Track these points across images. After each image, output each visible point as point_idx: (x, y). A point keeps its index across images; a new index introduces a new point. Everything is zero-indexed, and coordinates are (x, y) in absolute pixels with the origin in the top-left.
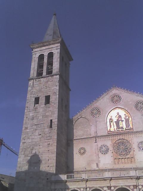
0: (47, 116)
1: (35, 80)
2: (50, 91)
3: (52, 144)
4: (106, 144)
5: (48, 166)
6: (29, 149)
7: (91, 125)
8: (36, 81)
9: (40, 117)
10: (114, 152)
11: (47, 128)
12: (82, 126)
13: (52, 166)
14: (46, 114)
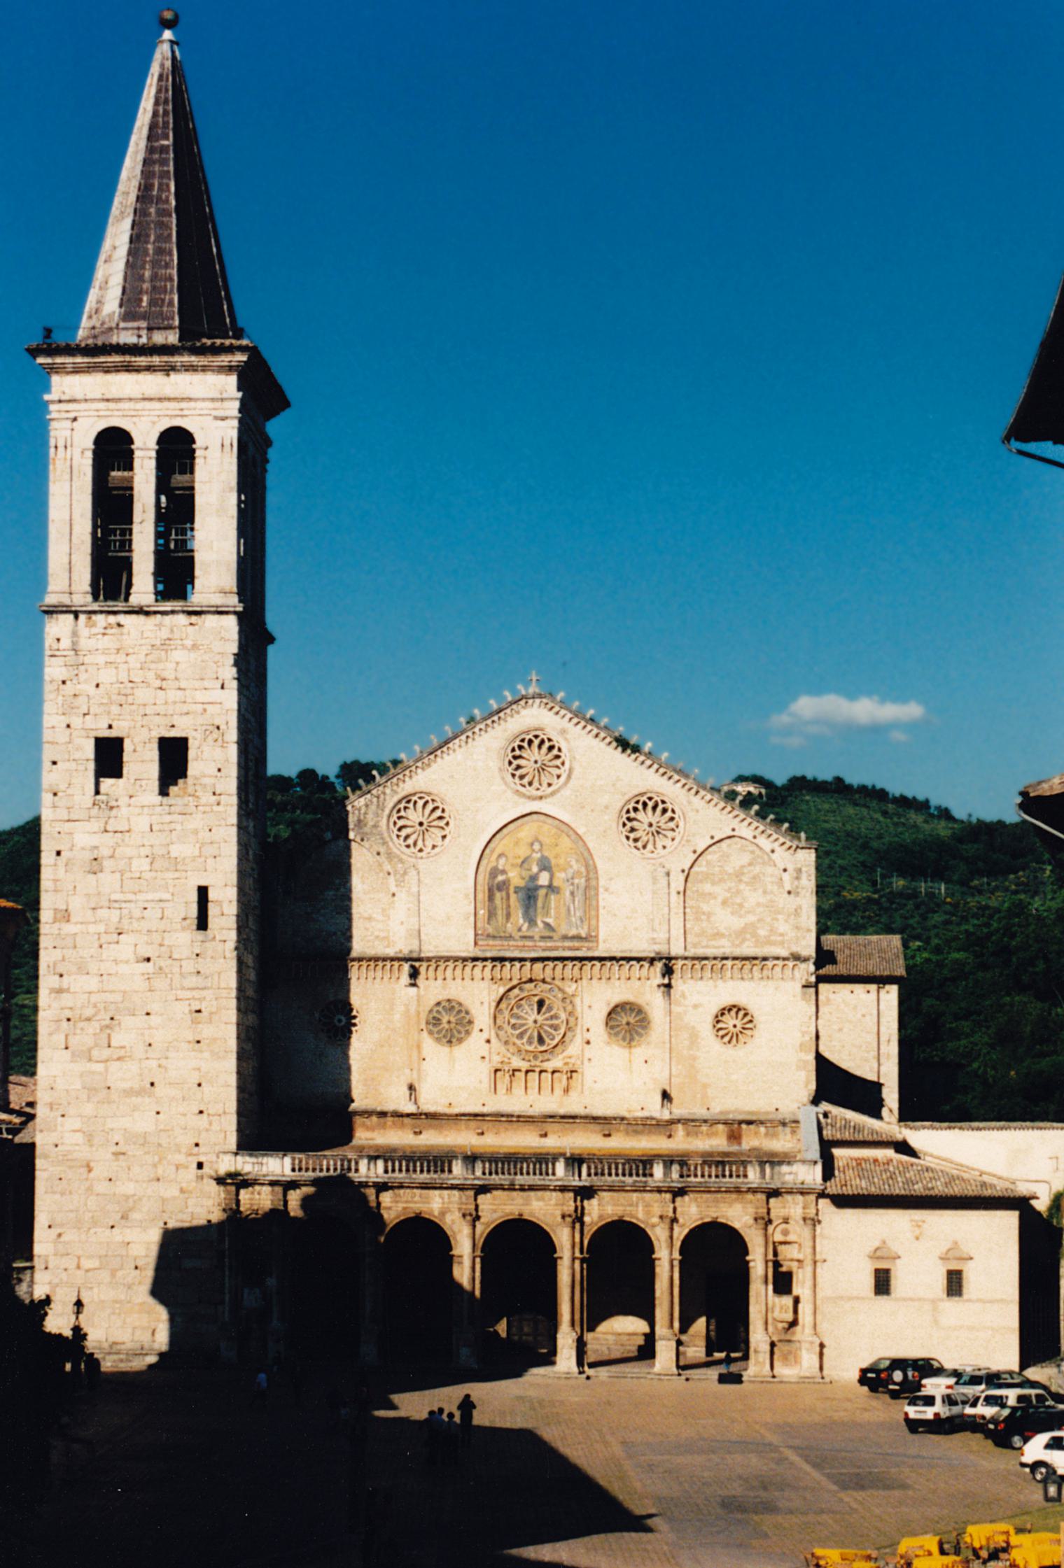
0: (175, 864)
1: (82, 617)
2: (185, 708)
3: (211, 1013)
5: (201, 1112)
6: (94, 1027)
8: (94, 625)
9: (135, 863)
10: (494, 1040)
11: (183, 929)
13: (221, 1111)
14: (172, 848)
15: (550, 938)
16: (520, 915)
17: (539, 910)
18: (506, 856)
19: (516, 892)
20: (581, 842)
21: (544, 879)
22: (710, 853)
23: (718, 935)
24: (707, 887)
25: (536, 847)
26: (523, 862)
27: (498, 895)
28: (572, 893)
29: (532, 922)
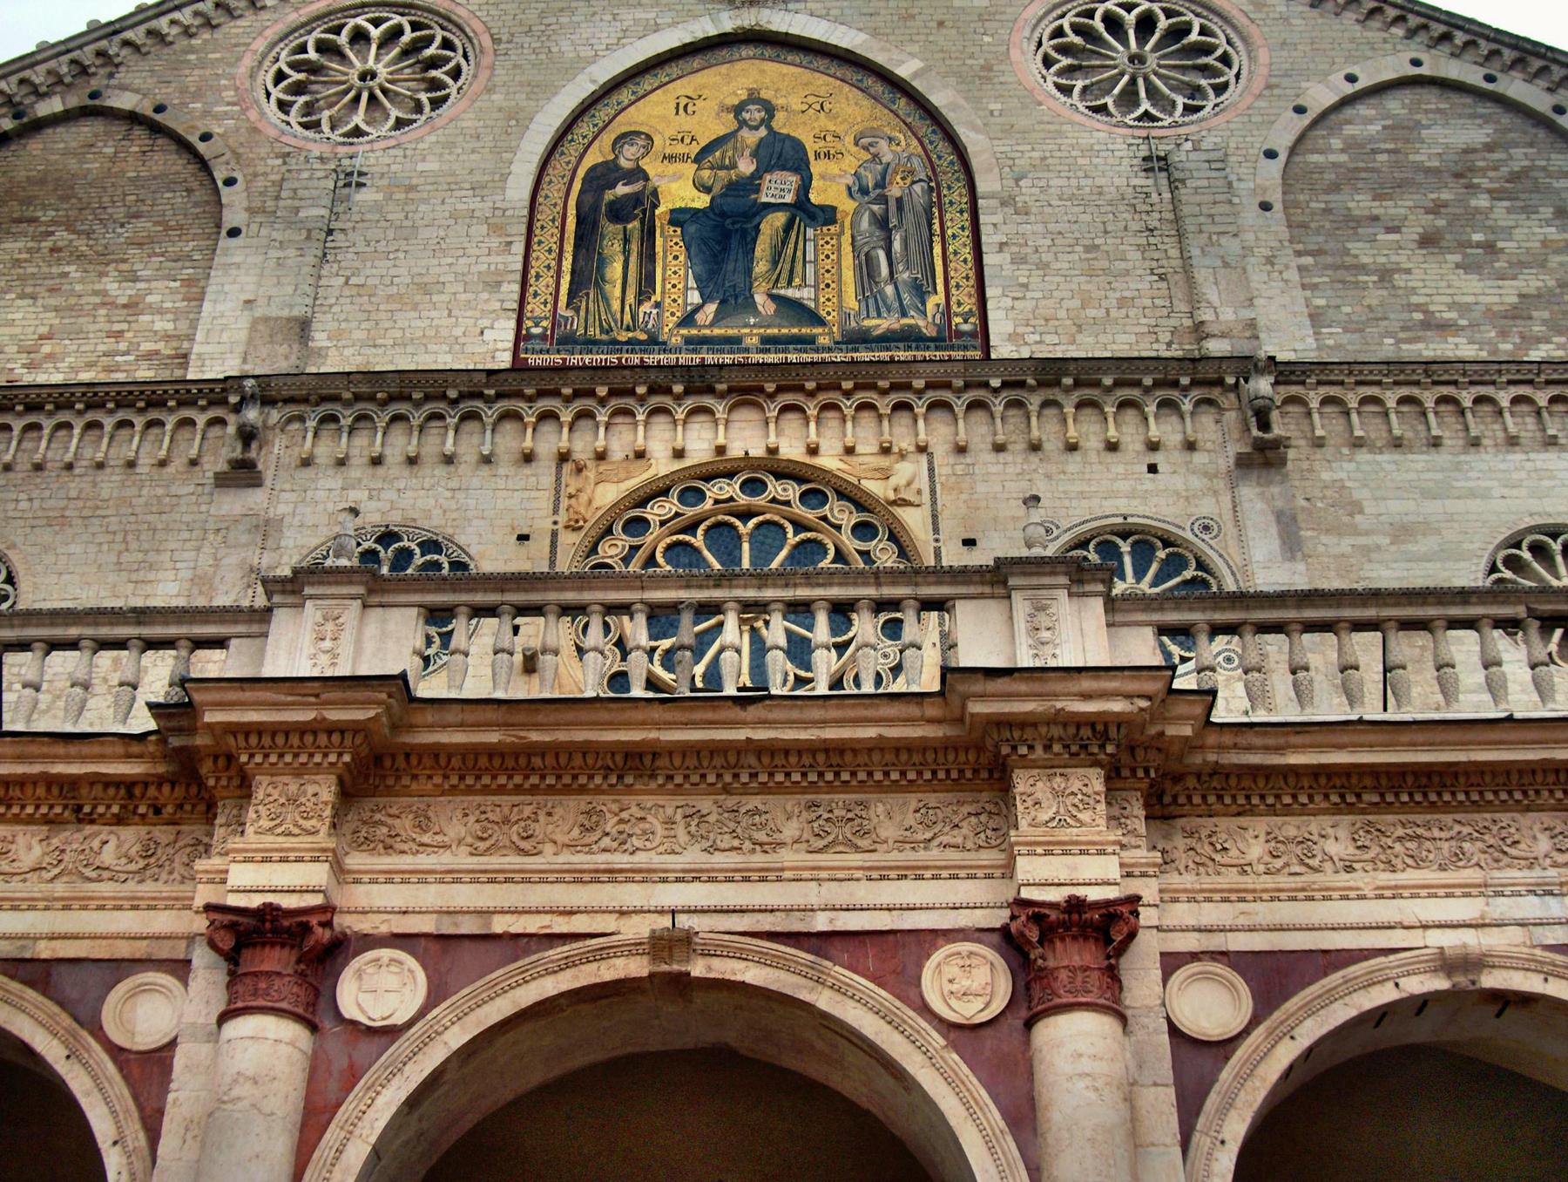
4: (435, 522)
7: (231, 218)
12: (62, 236)
15: (807, 342)
16: (692, 283)
17: (761, 267)
18: (649, 138)
19: (672, 222)
20: (903, 101)
21: (778, 188)
22: (1349, 122)
23: (1434, 326)
24: (1361, 203)
25: (754, 114)
26: (707, 150)
27: (611, 229)
28: (882, 223)
29: (734, 300)
